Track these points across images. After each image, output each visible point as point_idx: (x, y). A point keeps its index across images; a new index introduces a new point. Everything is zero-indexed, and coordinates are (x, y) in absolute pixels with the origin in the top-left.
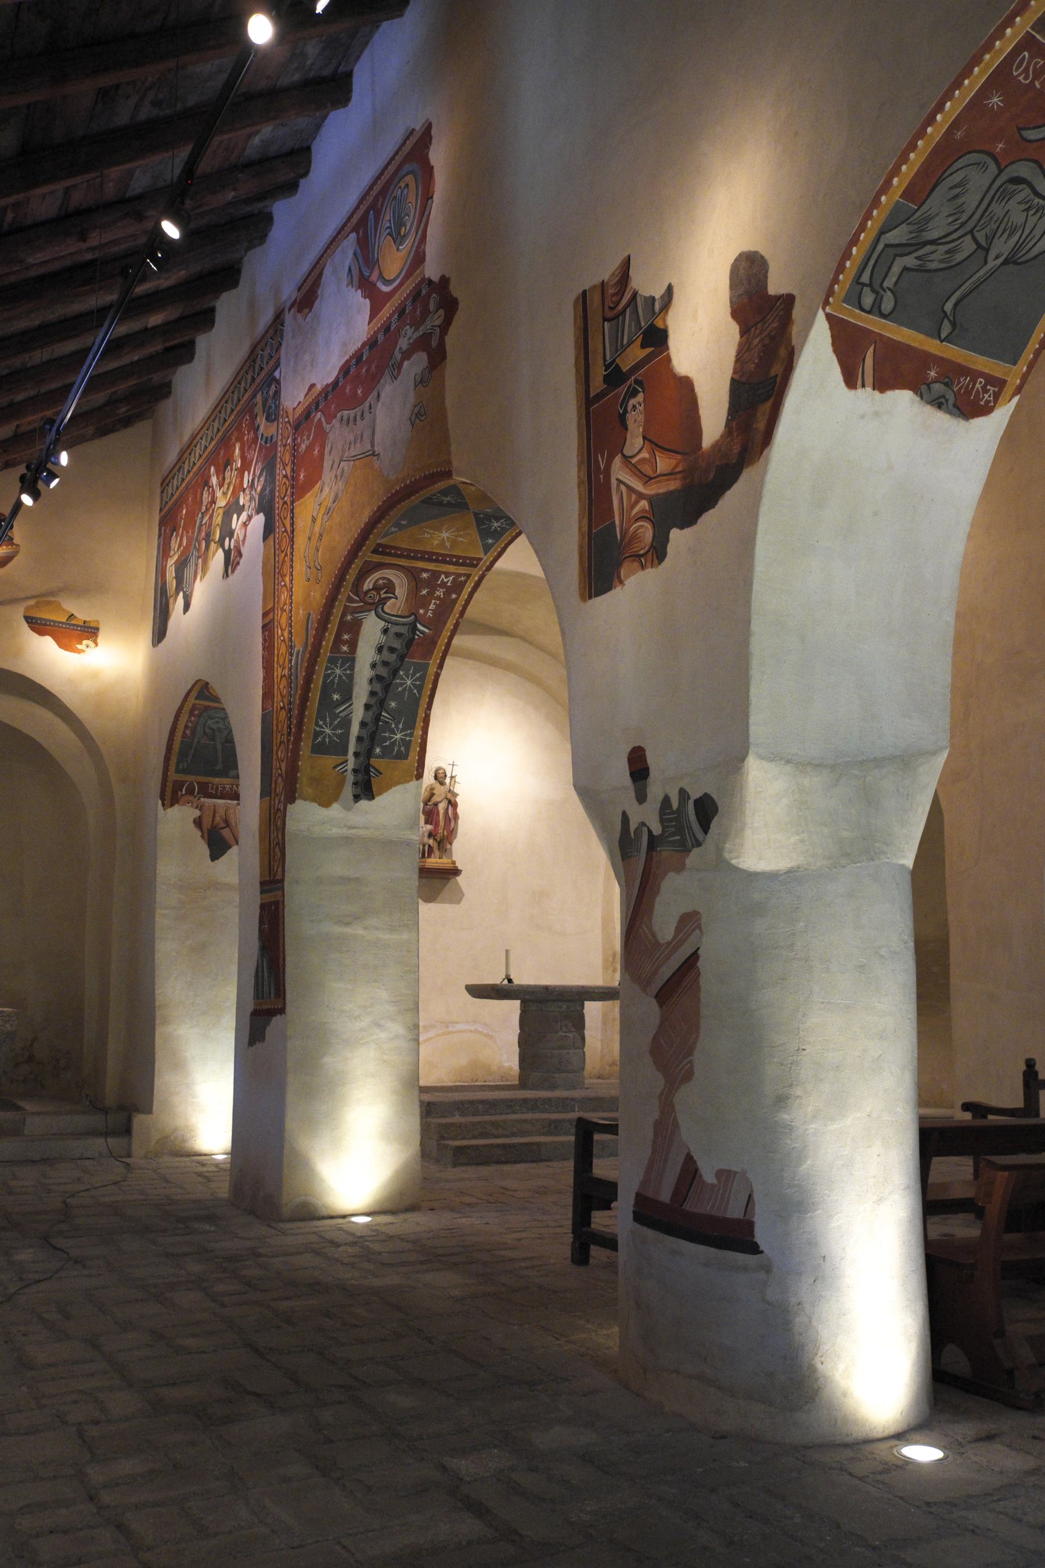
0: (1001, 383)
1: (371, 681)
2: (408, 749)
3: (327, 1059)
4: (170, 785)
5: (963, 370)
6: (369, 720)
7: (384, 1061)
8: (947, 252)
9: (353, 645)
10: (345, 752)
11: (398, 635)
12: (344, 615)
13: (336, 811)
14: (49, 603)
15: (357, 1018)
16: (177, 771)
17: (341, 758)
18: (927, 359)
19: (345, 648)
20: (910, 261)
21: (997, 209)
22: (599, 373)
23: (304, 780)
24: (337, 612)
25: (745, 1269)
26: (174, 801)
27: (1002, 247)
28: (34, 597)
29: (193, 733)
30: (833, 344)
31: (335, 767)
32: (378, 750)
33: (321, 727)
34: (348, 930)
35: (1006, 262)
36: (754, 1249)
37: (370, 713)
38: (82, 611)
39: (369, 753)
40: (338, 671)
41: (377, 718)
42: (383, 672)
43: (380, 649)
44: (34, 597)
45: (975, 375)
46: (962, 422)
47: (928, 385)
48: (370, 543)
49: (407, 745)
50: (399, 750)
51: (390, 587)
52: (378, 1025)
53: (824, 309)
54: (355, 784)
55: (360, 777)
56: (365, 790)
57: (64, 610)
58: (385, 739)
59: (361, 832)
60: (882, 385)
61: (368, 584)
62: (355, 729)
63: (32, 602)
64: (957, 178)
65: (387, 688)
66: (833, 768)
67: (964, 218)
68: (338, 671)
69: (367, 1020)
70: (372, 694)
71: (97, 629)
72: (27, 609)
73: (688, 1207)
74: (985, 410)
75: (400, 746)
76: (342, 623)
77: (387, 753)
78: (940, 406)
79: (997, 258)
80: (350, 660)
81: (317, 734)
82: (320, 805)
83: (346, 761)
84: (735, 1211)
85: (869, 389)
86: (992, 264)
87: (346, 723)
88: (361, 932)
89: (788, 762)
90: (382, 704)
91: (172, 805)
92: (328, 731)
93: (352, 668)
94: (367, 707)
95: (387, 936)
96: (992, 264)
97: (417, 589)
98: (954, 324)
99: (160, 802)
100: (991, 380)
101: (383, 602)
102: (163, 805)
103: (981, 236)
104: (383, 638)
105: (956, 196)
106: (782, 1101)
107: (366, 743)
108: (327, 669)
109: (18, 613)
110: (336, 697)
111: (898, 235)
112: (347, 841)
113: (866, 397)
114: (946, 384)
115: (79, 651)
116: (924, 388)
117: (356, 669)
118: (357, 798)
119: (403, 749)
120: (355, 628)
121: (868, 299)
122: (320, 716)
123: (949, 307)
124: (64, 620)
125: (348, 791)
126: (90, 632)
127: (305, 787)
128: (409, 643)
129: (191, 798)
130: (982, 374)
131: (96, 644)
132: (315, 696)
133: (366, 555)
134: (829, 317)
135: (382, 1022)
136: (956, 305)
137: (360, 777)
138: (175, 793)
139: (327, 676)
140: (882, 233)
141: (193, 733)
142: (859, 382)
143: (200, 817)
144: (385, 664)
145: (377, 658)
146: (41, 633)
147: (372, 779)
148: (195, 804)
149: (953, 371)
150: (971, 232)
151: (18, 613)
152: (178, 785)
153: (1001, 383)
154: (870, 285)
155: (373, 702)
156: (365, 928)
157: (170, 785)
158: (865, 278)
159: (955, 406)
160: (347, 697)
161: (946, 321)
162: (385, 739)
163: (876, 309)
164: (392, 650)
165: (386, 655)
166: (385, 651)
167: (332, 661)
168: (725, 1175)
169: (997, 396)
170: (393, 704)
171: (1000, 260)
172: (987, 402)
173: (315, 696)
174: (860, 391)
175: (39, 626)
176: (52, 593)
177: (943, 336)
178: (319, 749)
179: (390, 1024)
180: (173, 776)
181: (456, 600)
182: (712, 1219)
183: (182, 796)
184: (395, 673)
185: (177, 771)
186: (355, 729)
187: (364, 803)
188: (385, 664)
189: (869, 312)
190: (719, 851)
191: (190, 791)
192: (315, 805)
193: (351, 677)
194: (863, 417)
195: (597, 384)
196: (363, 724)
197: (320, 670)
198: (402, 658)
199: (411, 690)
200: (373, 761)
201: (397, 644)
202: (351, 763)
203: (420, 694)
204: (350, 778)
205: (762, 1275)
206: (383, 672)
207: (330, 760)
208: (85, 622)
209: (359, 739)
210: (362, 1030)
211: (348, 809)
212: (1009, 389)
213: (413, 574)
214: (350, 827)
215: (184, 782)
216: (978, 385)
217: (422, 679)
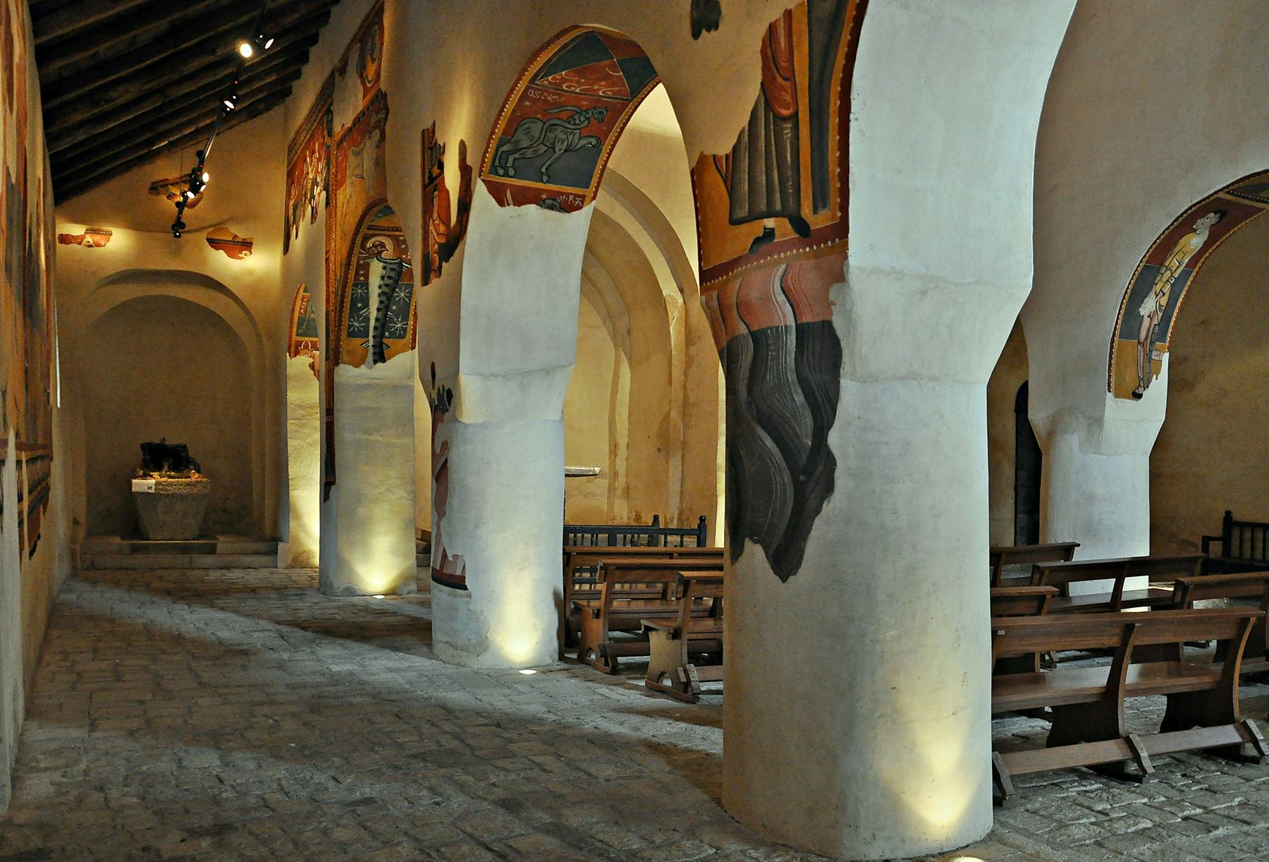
0: (583, 197)
1: (379, 295)
2: (405, 333)
3: (361, 510)
4: (293, 343)
5: (562, 194)
6: (380, 317)
7: (395, 511)
8: (534, 151)
9: (367, 276)
10: (368, 336)
11: (392, 269)
12: (358, 261)
13: (363, 369)
14: (222, 229)
15: (377, 487)
16: (298, 335)
17: (364, 340)
18: (540, 191)
19: (362, 278)
20: (517, 155)
21: (551, 135)
22: (427, 175)
23: (344, 352)
24: (354, 259)
25: (462, 596)
26: (297, 353)
27: (560, 147)
28: (211, 226)
29: (306, 311)
30: (488, 190)
31: (362, 345)
32: (387, 334)
33: (352, 322)
34: (372, 438)
35: (566, 151)
36: (465, 588)
37: (381, 313)
38: (241, 233)
39: (382, 335)
40: (359, 291)
41: (386, 315)
42: (386, 289)
43: (383, 278)
44: (211, 226)
45: (568, 195)
46: (567, 214)
47: (544, 202)
48: (365, 225)
49: (405, 330)
50: (400, 334)
51: (382, 245)
52: (388, 490)
53: (480, 177)
54: (374, 353)
55: (377, 350)
56: (380, 357)
57: (230, 233)
58: (391, 327)
59: (378, 381)
60: (518, 203)
61: (369, 245)
62: (372, 323)
63: (211, 229)
64: (525, 127)
65: (389, 299)
66: (504, 377)
67: (536, 138)
68: (359, 291)
69: (383, 489)
70: (381, 302)
71: (252, 243)
72: (209, 233)
73: (444, 571)
74: (579, 208)
75: (400, 331)
76: (358, 265)
77: (392, 335)
78: (552, 209)
79: (560, 150)
80: (366, 285)
81: (350, 326)
82: (354, 366)
83: (368, 341)
84: (459, 573)
85: (512, 206)
86: (558, 153)
87: (367, 319)
88: (379, 438)
89: (480, 375)
90: (387, 308)
91: (295, 356)
92: (357, 324)
93: (367, 289)
94: (378, 310)
95: (393, 441)
96: (558, 153)
97: (399, 246)
98: (549, 177)
99: (288, 354)
100: (576, 196)
101: (380, 253)
102: (290, 355)
103: (548, 144)
104: (384, 272)
105: (528, 132)
106: (477, 526)
107: (380, 329)
108: (353, 290)
109: (203, 236)
110: (359, 305)
111: (505, 148)
113: (511, 210)
114: (553, 200)
115: (240, 258)
116: (541, 203)
117: (370, 289)
118: (375, 362)
119: (402, 332)
120: (366, 267)
121: (501, 172)
122: (351, 315)
123: (543, 170)
124: (231, 239)
125: (370, 357)
126: (247, 245)
128: (400, 274)
129: (307, 351)
130: (572, 194)
131: (251, 253)
132: (347, 305)
133: (364, 230)
134: (483, 180)
135: (392, 490)
136: (547, 169)
137: (377, 350)
138: (297, 348)
139: (353, 294)
140: (497, 150)
141: (306, 311)
142: (506, 203)
143: (313, 363)
144: (386, 285)
145: (382, 282)
146: (217, 248)
147: (385, 351)
148: (310, 355)
149: (554, 195)
150: (542, 143)
151: (203, 236)
152: (298, 344)
153: (583, 197)
154: (500, 166)
156: (381, 436)
157: (293, 343)
158: (497, 163)
159: (560, 208)
160: (366, 305)
161: (544, 176)
162: (391, 327)
163: (506, 175)
164: (389, 278)
165: (387, 281)
166: (386, 279)
167: (355, 285)
168: (456, 557)
169: (582, 203)
170: (394, 307)
171: (562, 151)
172: (578, 205)
173: (347, 305)
174: (507, 207)
175: (215, 244)
176: (224, 222)
177: (545, 181)
178: (351, 335)
180: (295, 338)
182: (452, 576)
183: (301, 350)
184: (393, 290)
185: (298, 335)
186: (372, 323)
187: (380, 365)
188: (386, 285)
189: (503, 176)
190: (454, 414)
191: (306, 347)
192: (351, 367)
193: (368, 293)
194: (512, 217)
195: (427, 182)
196: (377, 319)
197: (349, 290)
198: (396, 281)
199: (404, 300)
200: (385, 340)
201: (393, 274)
203: (410, 301)
204: (371, 350)
205: (468, 599)
206: (386, 289)
207: (359, 341)
208: (244, 239)
209: (375, 328)
210: (381, 494)
211: (370, 368)
212: (588, 199)
214: (371, 379)
215: (301, 342)
216: (570, 199)
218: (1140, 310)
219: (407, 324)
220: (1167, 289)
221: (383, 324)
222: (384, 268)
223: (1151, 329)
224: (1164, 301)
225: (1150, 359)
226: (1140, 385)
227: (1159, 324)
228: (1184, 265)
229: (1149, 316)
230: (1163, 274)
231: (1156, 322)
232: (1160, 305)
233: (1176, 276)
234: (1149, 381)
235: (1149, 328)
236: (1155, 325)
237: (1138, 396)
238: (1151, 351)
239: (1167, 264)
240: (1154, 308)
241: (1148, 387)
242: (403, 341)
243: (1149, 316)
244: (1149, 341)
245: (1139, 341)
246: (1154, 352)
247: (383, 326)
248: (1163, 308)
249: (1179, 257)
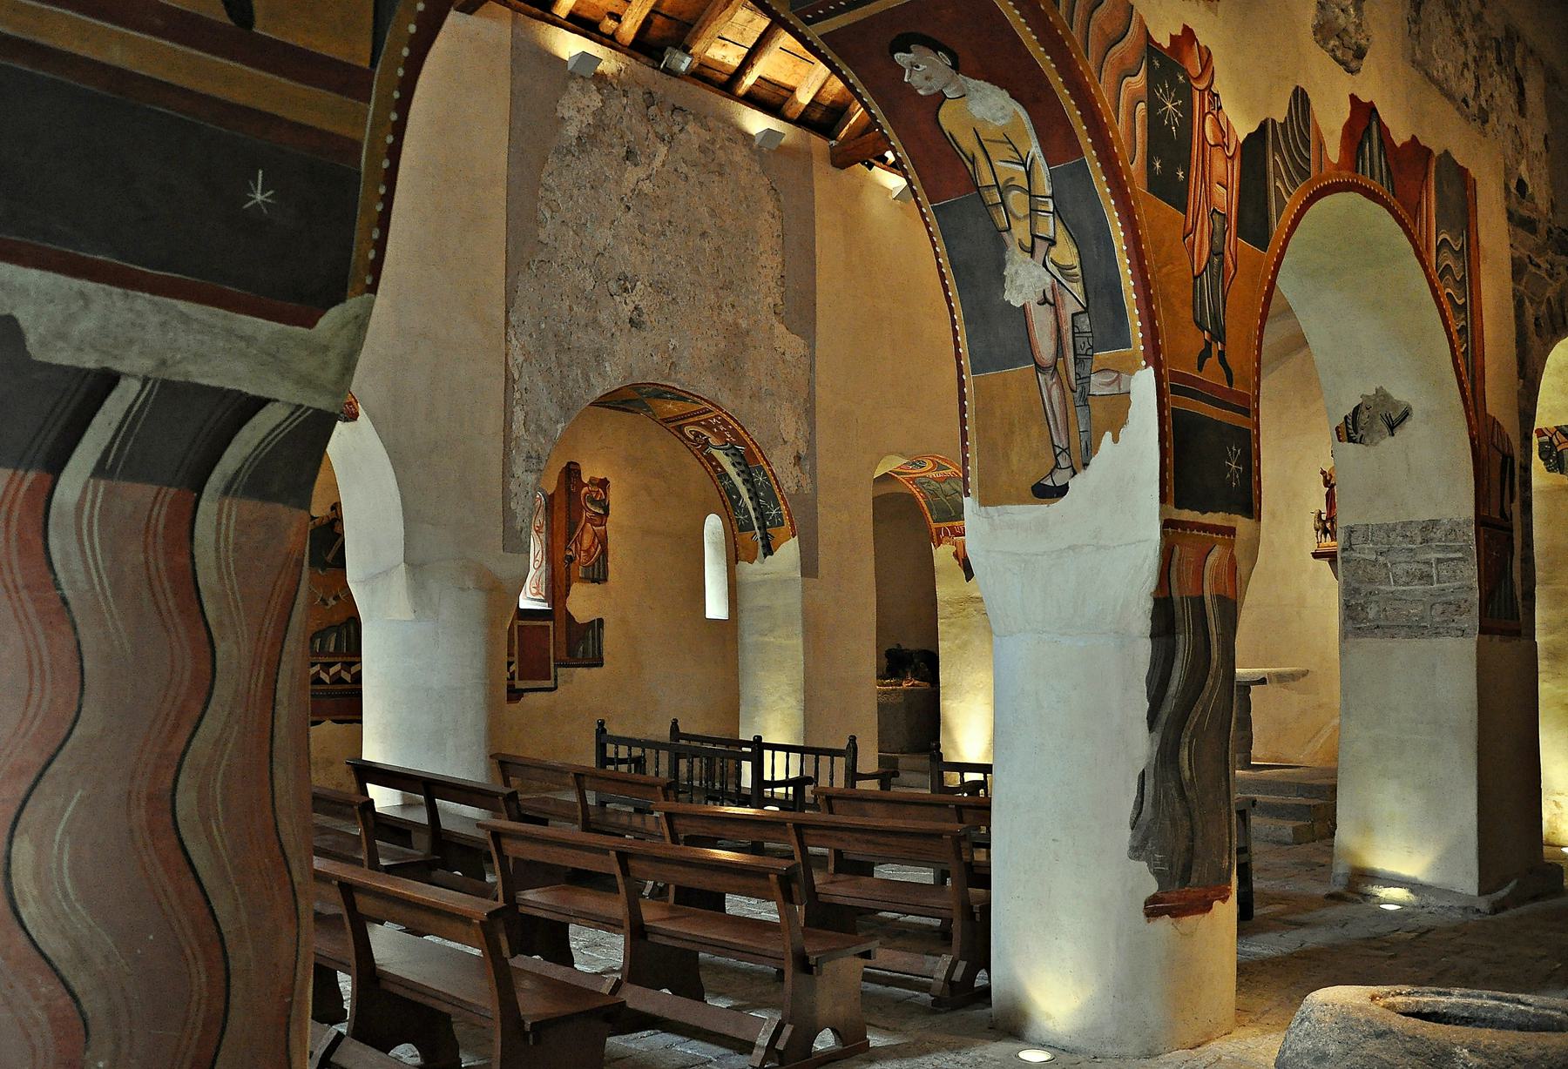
6: (755, 506)
34: (766, 639)
37: (754, 502)
56: (769, 550)
65: (753, 485)
70: (749, 490)
80: (725, 475)
90: (756, 494)
94: (751, 498)
112: (764, 582)
118: (765, 556)
125: (760, 551)
127: (742, 554)
138: (938, 534)
155: (751, 495)
160: (740, 497)
164: (739, 463)
178: (741, 529)
179: (788, 699)
181: (733, 428)
186: (753, 514)
193: (733, 483)
196: (754, 509)
198: (746, 466)
202: (759, 535)
204: (760, 543)
207: (749, 534)
209: (757, 518)
213: (697, 424)
217: (765, 474)
218: (1007, 297)
219: (780, 510)
220: (1048, 226)
221: (762, 517)
222: (727, 455)
223: (1067, 327)
224: (1066, 253)
225: (1085, 397)
226: (1057, 465)
227: (1086, 310)
228: (1041, 161)
229: (1044, 301)
230: (1003, 203)
231: (1070, 307)
232: (1061, 268)
233: (1049, 192)
234: (1090, 450)
235: (1059, 329)
236: (1073, 315)
237: (1047, 492)
238: (1084, 380)
239: (986, 178)
240: (1048, 279)
241: (1086, 465)
242: (782, 529)
243: (1044, 301)
244: (1070, 356)
245: (1039, 368)
246: (1093, 377)
247: (762, 514)
248: (1077, 270)
249: (999, 153)
